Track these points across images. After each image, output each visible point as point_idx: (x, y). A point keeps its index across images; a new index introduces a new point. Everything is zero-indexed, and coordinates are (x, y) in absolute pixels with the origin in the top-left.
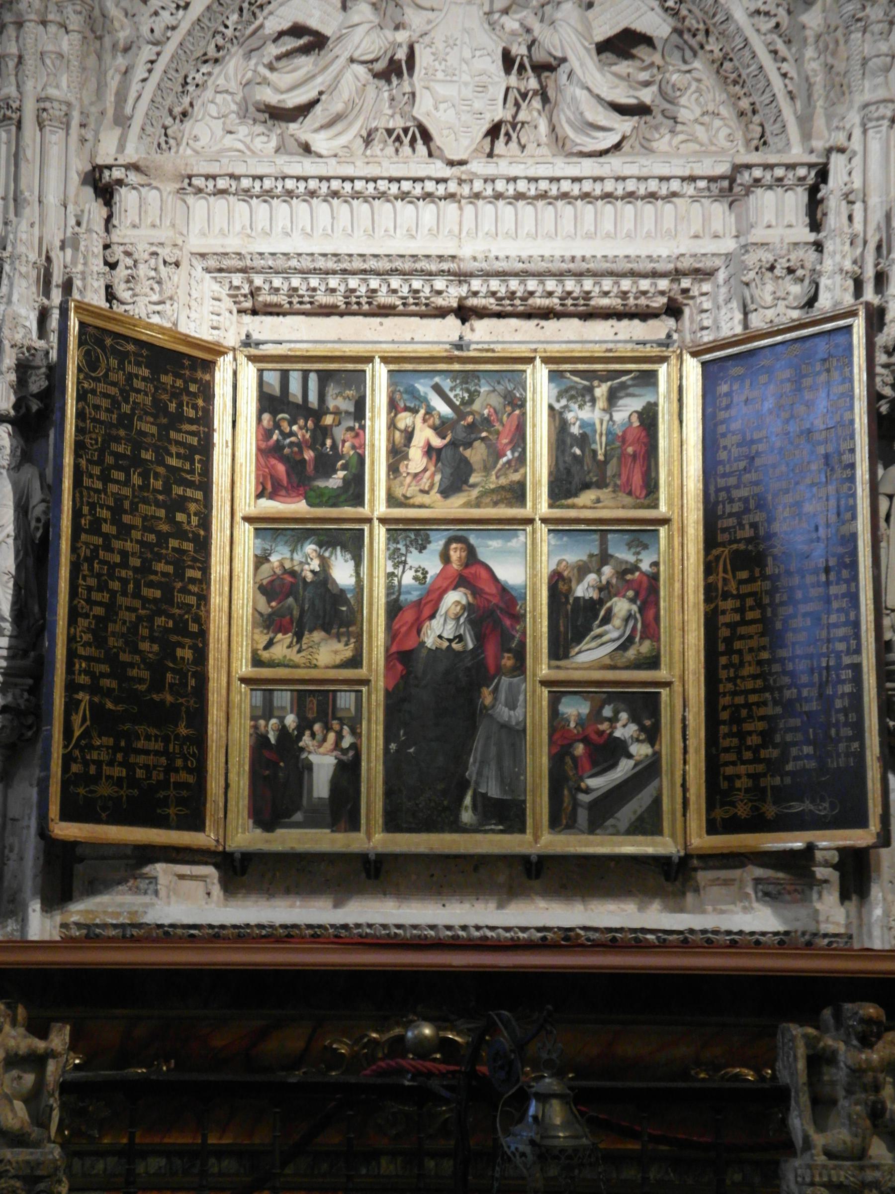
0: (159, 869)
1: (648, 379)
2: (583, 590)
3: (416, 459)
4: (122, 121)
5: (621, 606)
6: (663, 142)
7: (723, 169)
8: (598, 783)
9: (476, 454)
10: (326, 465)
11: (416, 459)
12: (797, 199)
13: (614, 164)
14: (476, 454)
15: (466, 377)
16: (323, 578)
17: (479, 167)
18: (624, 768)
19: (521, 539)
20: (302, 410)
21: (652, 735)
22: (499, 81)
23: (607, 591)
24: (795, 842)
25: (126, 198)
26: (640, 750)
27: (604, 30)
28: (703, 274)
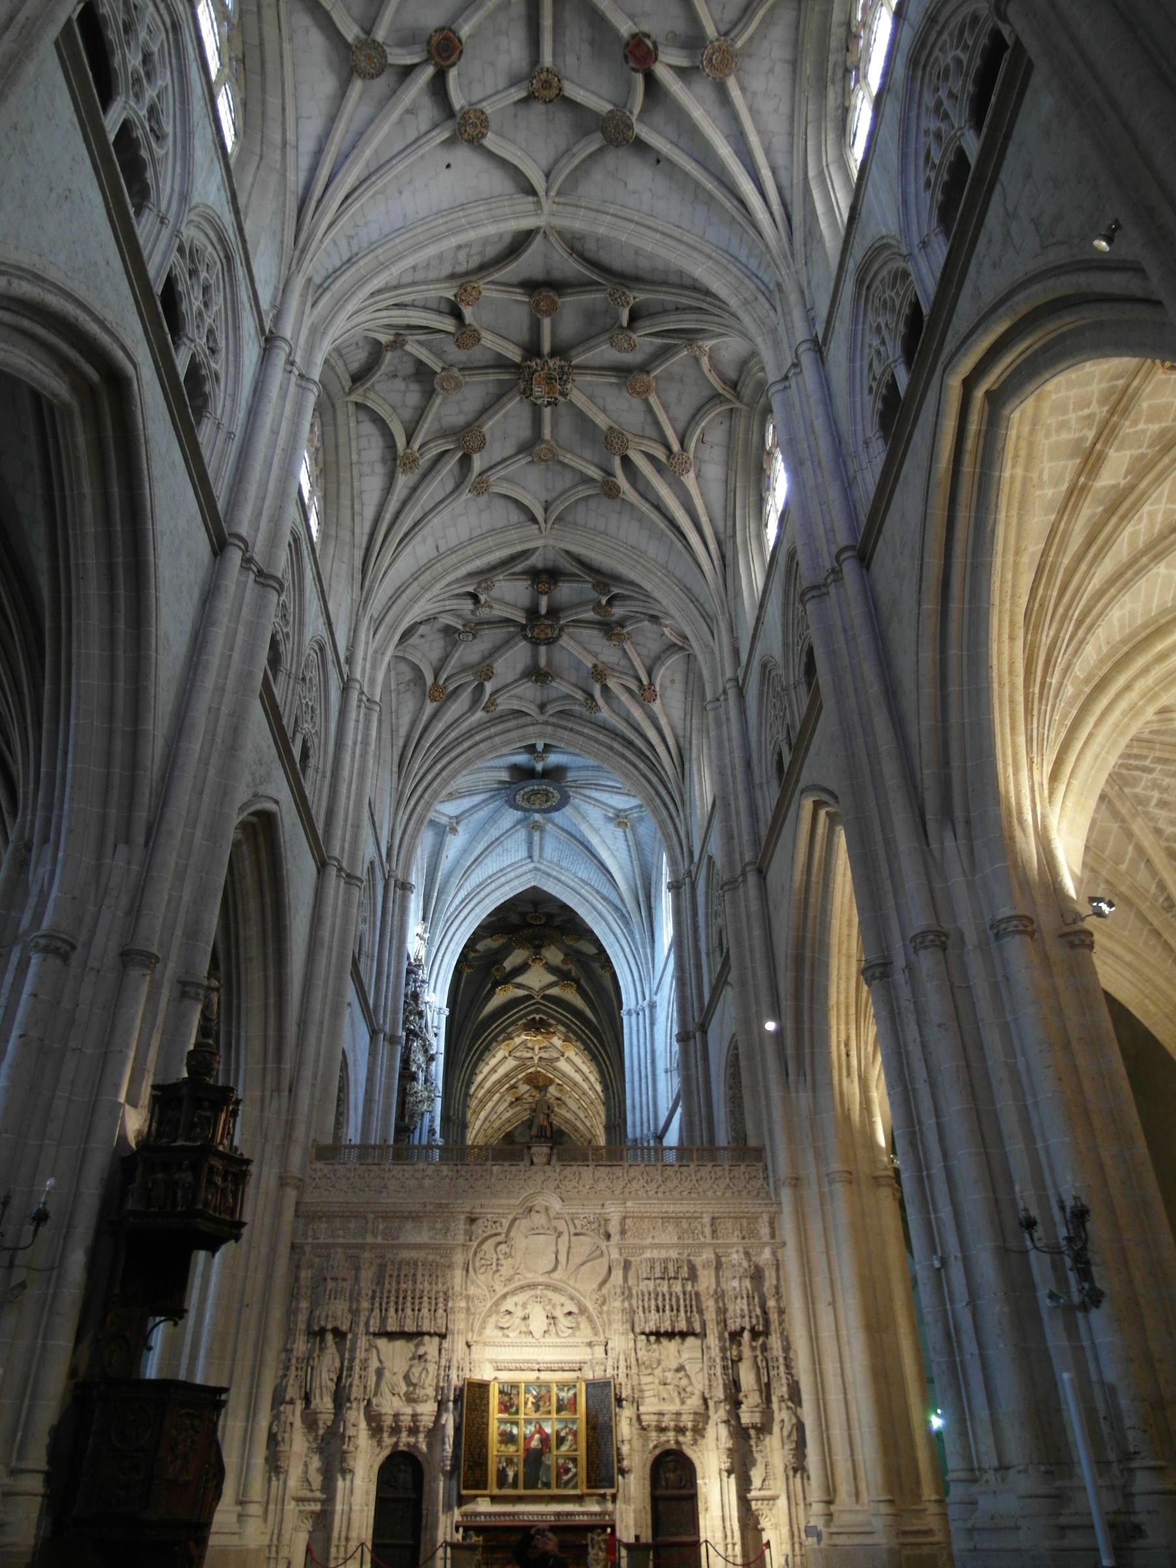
0: (479, 1500)
1: (575, 1386)
2: (563, 1434)
3: (530, 1405)
4: (472, 1330)
5: (570, 1437)
6: (577, 1333)
7: (588, 1340)
8: (565, 1478)
9: (541, 1403)
10: (511, 1406)
11: (530, 1405)
12: (602, 1348)
13: (568, 1340)
14: (541, 1403)
15: (539, 1386)
16: (511, 1432)
17: (542, 1340)
18: (570, 1475)
19: (550, 1423)
20: (507, 1394)
21: (576, 1467)
22: (546, 1321)
23: (567, 1434)
24: (602, 1491)
25: (473, 1348)
26: (574, 1470)
27: (566, 1311)
28: (585, 1363)
